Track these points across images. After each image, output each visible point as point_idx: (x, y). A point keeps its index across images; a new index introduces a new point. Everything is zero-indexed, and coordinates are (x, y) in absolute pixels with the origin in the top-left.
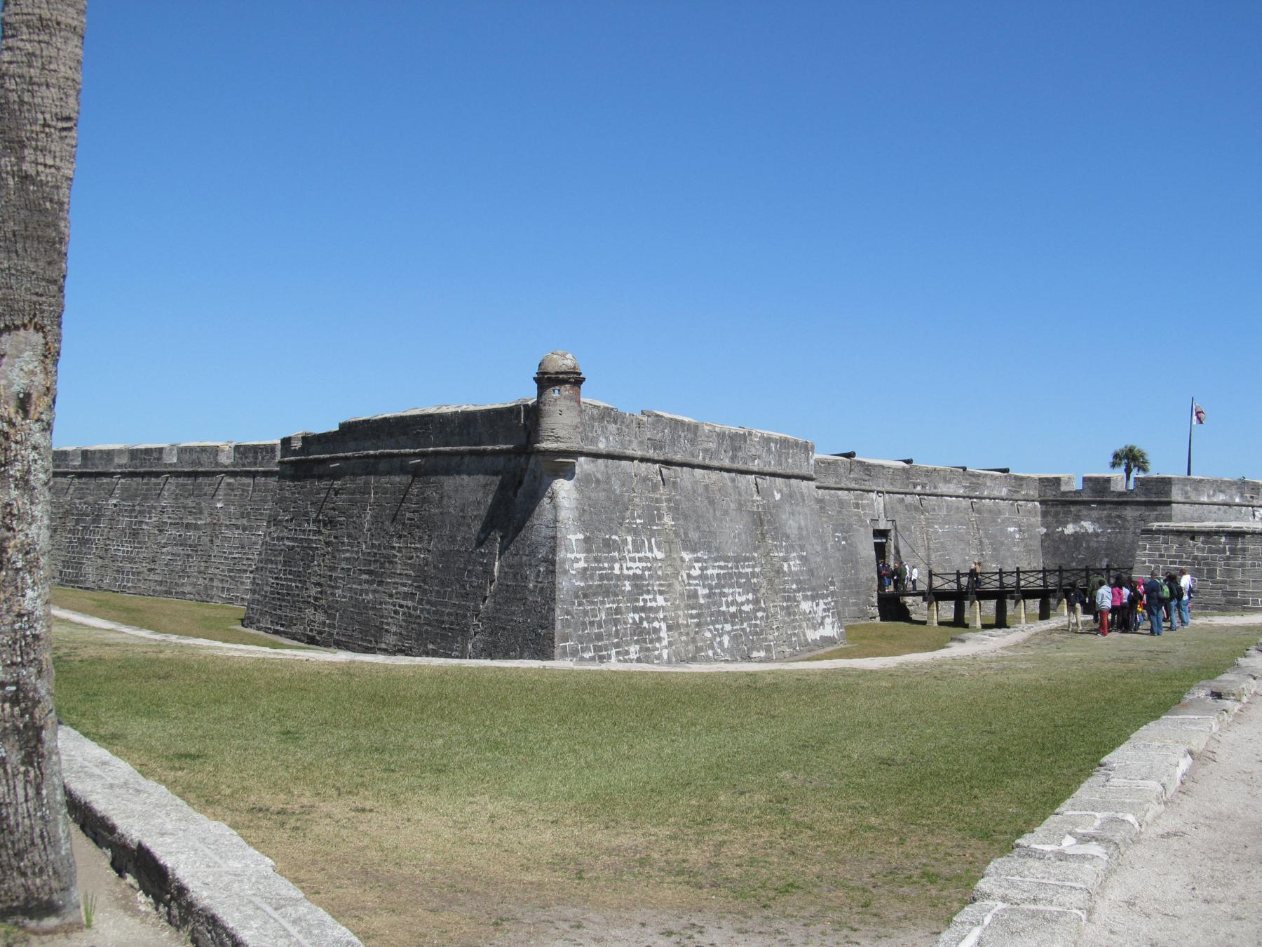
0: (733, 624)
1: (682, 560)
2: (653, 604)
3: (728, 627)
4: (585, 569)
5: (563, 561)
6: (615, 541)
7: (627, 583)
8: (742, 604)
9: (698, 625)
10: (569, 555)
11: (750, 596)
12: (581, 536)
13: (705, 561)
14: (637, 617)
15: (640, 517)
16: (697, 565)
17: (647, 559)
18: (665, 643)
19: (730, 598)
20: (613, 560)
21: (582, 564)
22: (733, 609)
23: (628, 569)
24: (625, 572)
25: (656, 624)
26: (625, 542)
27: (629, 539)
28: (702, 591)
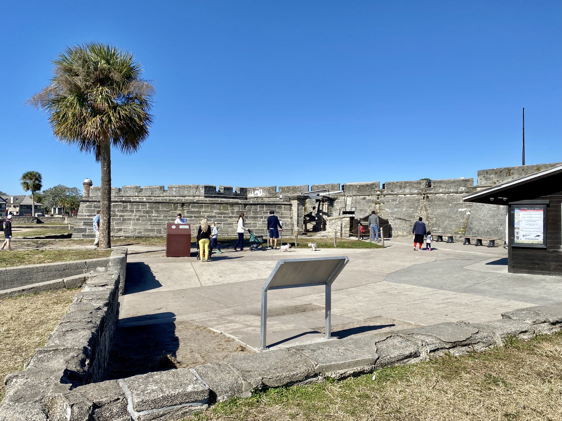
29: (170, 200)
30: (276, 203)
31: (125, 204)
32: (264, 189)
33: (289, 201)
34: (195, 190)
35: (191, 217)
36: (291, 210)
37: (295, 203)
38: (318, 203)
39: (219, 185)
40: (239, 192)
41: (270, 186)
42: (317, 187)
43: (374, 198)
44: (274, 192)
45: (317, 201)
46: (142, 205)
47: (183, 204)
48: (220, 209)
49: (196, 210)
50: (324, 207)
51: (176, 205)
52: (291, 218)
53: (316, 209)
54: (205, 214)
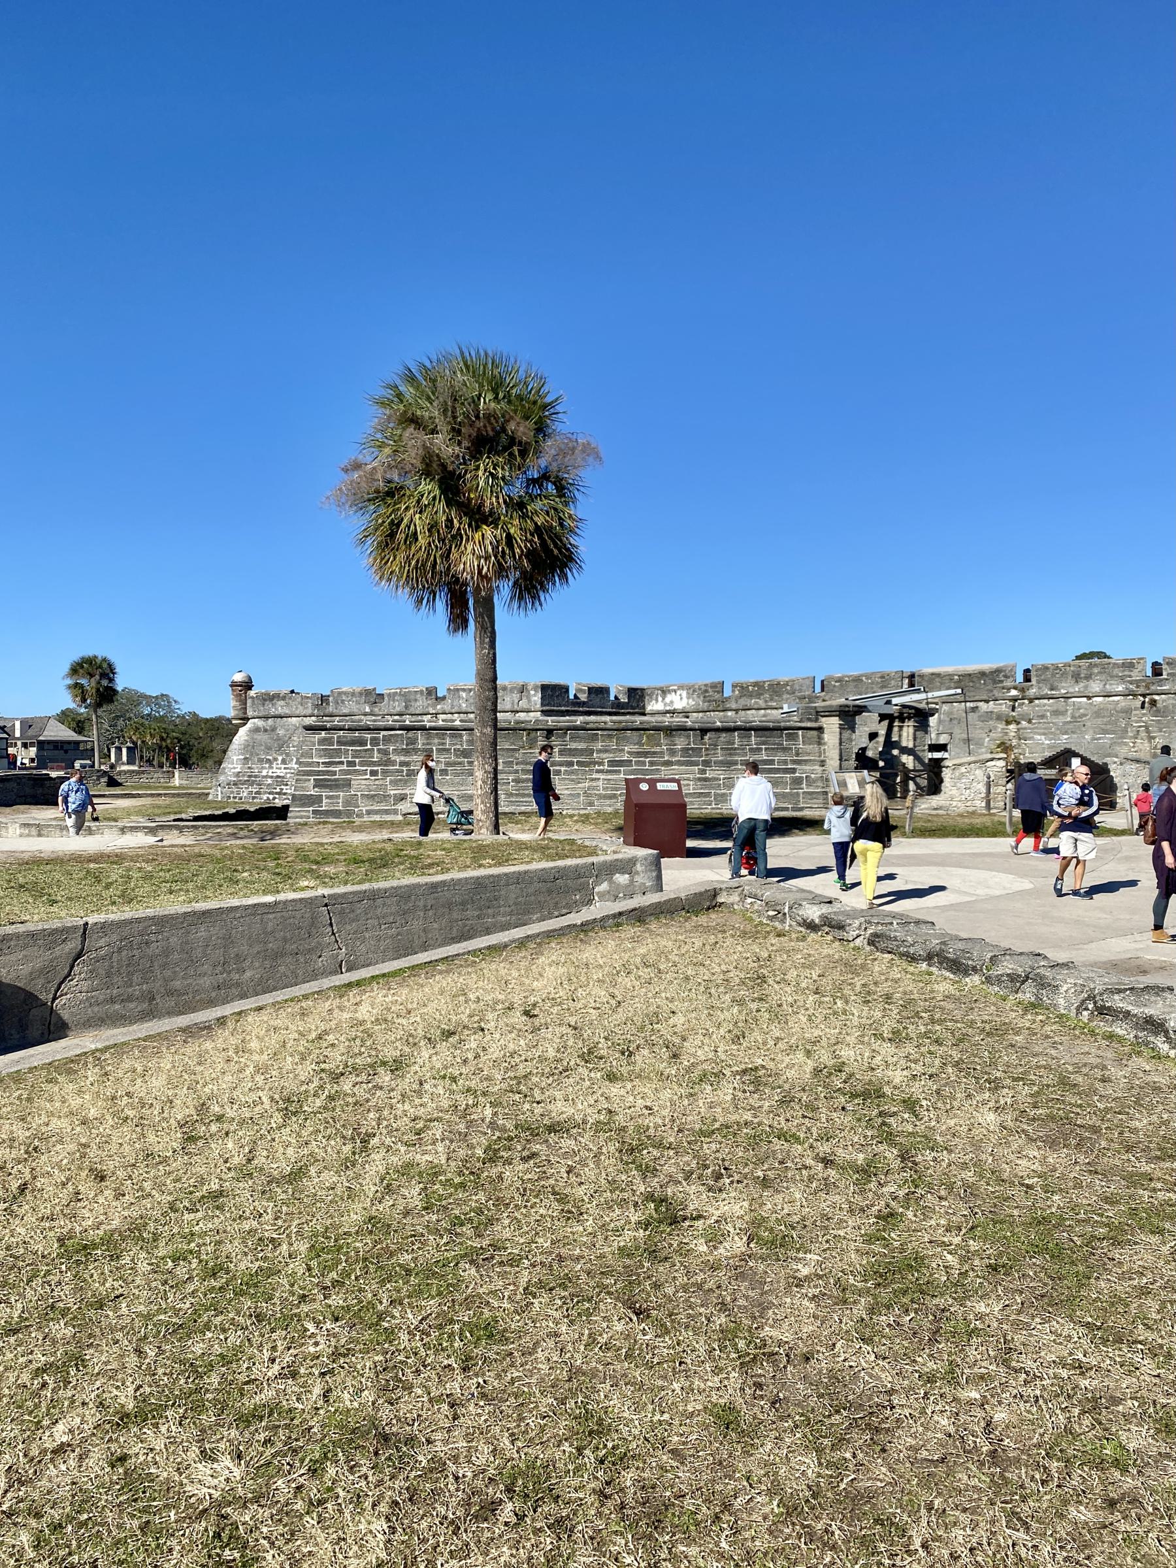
26: (276, 759)
27: (280, 758)
29: (517, 722)
30: (782, 724)
31: (411, 734)
32: (691, 690)
33: (816, 720)
34: (516, 696)
35: (571, 764)
36: (820, 742)
37: (832, 725)
38: (886, 723)
39: (576, 682)
40: (624, 699)
41: (708, 682)
42: (839, 680)
43: (1003, 707)
44: (717, 696)
45: (883, 717)
46: (452, 736)
47: (550, 732)
48: (640, 743)
49: (581, 746)
50: (904, 734)
51: (533, 734)
52: (823, 763)
53: (881, 739)
54: (605, 756)
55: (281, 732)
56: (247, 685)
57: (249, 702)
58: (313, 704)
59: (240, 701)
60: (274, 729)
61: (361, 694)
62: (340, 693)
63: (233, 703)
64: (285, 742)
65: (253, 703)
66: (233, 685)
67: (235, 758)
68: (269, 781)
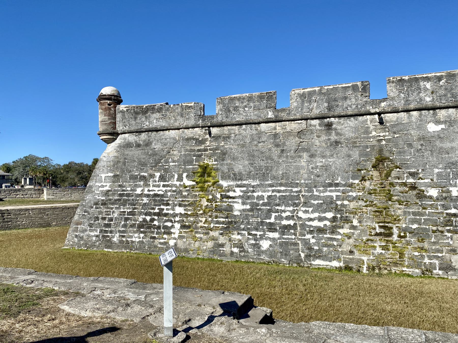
0: (283, 233)
1: (221, 187)
2: (171, 212)
3: (276, 235)
4: (109, 191)
5: (91, 187)
6: (144, 177)
7: (144, 198)
8: (311, 220)
9: (223, 229)
10: (97, 184)
11: (330, 215)
12: (112, 175)
13: (253, 187)
14: (148, 218)
15: (174, 162)
16: (237, 189)
17: (175, 186)
18: (176, 236)
19: (284, 215)
20: (136, 186)
21: (107, 188)
22: (285, 222)
23: (149, 191)
24: (146, 192)
25: (169, 224)
26: (152, 176)
27: (158, 175)
28: (238, 207)
55: (157, 146)
56: (116, 100)
57: (119, 116)
58: (196, 115)
59: (109, 115)
60: (148, 144)
61: (261, 97)
62: (232, 99)
63: (101, 117)
64: (162, 157)
65: (124, 118)
66: (102, 98)
67: (103, 176)
68: (145, 200)
